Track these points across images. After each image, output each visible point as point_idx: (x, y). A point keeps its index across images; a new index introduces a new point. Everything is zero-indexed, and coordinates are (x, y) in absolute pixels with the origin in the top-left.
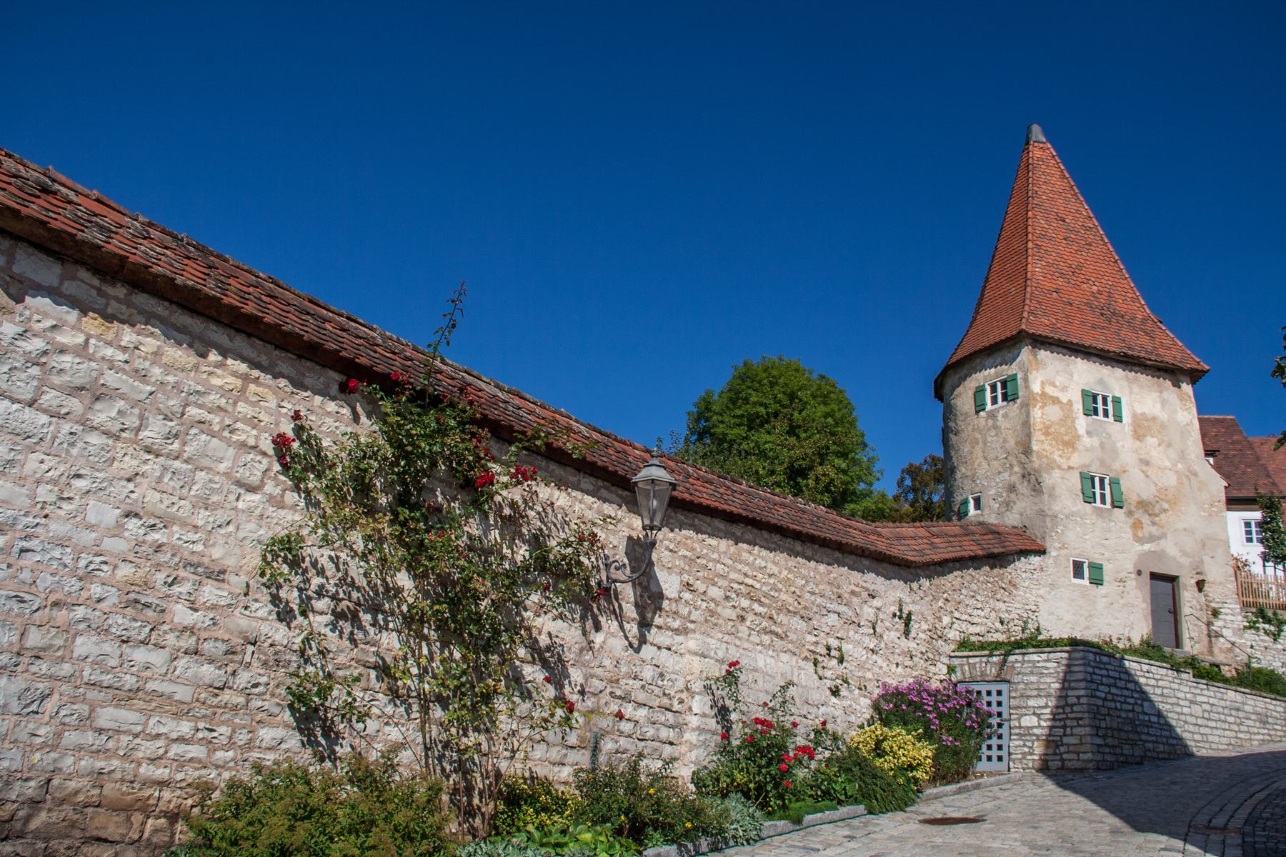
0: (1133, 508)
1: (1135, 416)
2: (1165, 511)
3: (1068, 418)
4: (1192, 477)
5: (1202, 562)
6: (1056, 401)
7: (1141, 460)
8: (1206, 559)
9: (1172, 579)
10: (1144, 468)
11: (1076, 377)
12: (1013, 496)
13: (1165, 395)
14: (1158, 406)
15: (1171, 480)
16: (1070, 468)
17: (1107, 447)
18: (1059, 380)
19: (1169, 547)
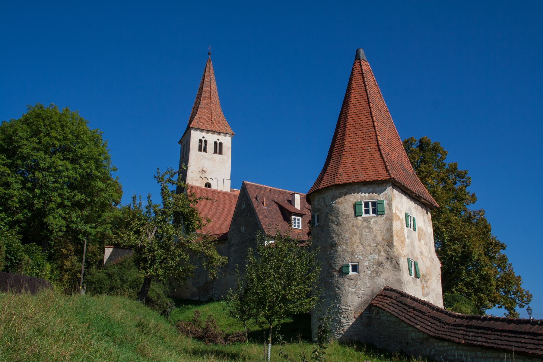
3: (402, 229)
12: (381, 269)
18: (399, 207)
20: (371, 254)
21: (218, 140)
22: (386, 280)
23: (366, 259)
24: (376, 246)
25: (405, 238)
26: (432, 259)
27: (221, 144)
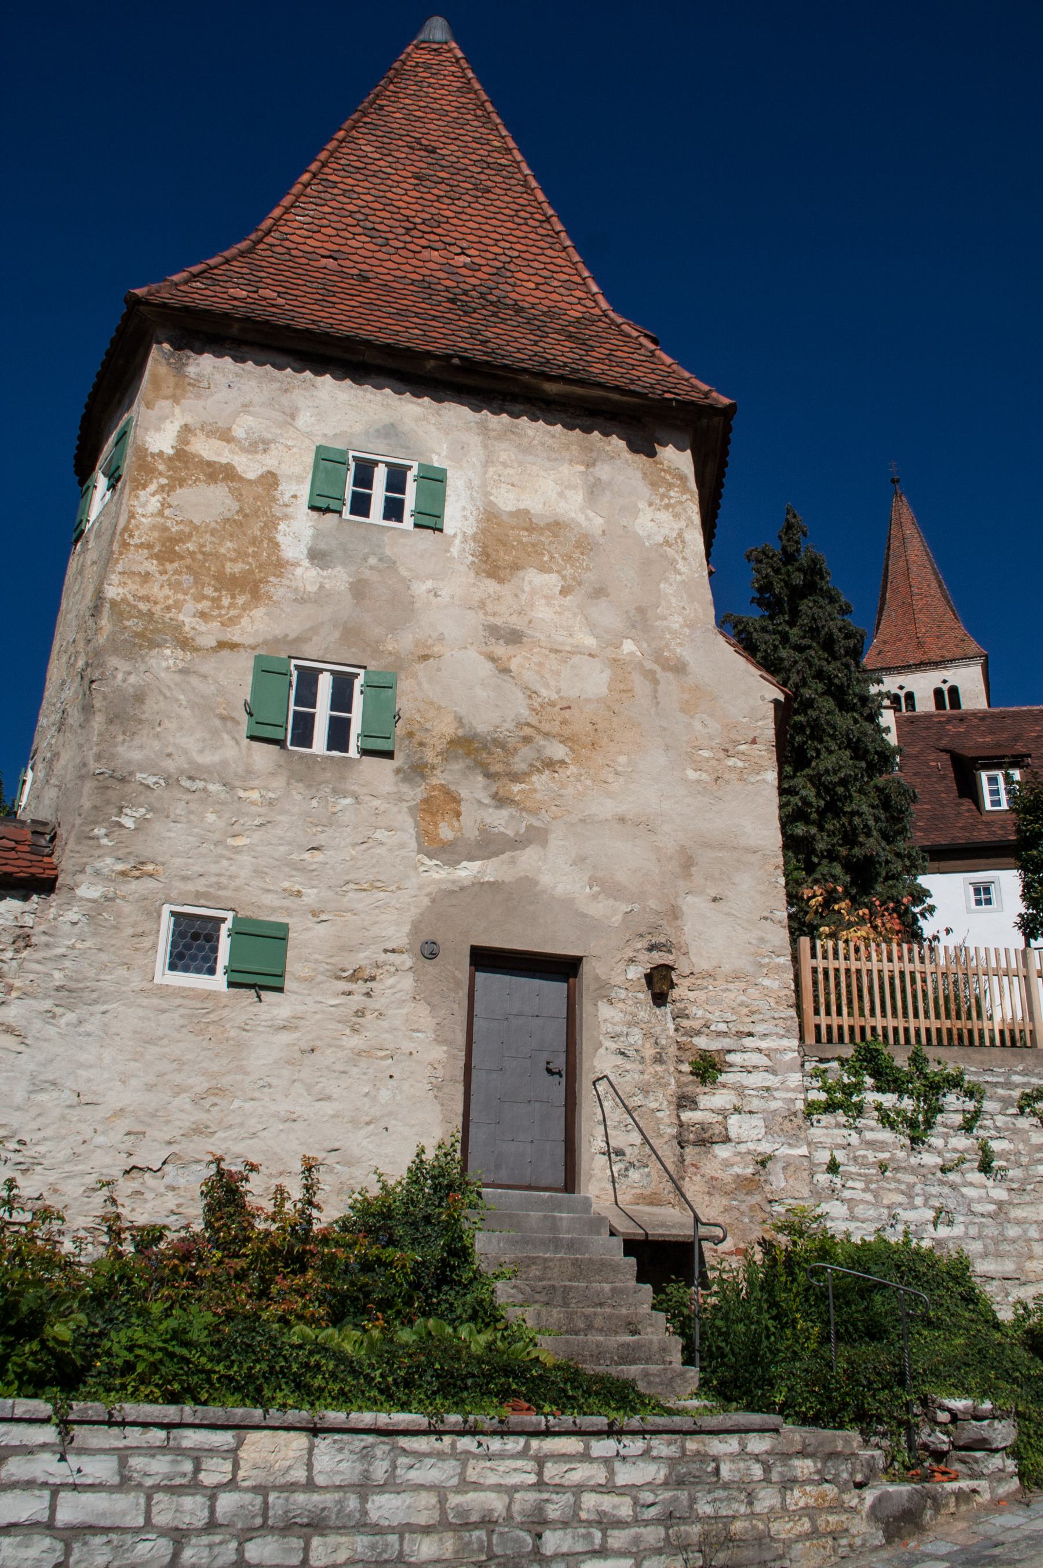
0: (430, 756)
2: (551, 765)
4: (666, 677)
5: (675, 913)
6: (220, 473)
7: (494, 631)
8: (694, 905)
9: (564, 968)
10: (500, 650)
11: (305, 419)
13: (603, 471)
14: (577, 497)
15: (593, 682)
17: (380, 596)
19: (556, 872)
21: (945, 682)
25: (280, 566)
27: (954, 691)
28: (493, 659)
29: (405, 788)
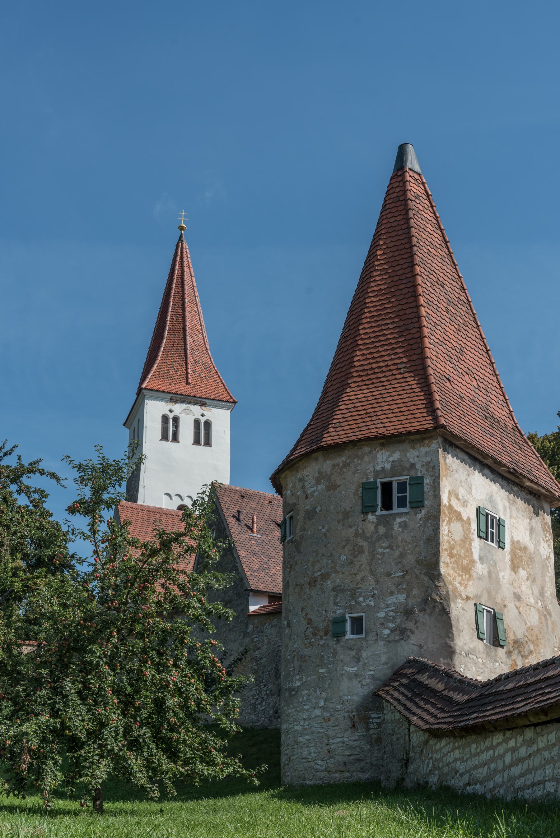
1: (513, 542)
3: (466, 540)
4: (548, 617)
7: (515, 594)
10: (517, 603)
12: (410, 625)
15: (534, 619)
16: (468, 598)
18: (462, 492)
20: (392, 593)
22: (421, 647)
23: (382, 605)
24: (403, 576)
25: (473, 562)
26: (547, 610)
28: (517, 608)
29: (507, 660)
